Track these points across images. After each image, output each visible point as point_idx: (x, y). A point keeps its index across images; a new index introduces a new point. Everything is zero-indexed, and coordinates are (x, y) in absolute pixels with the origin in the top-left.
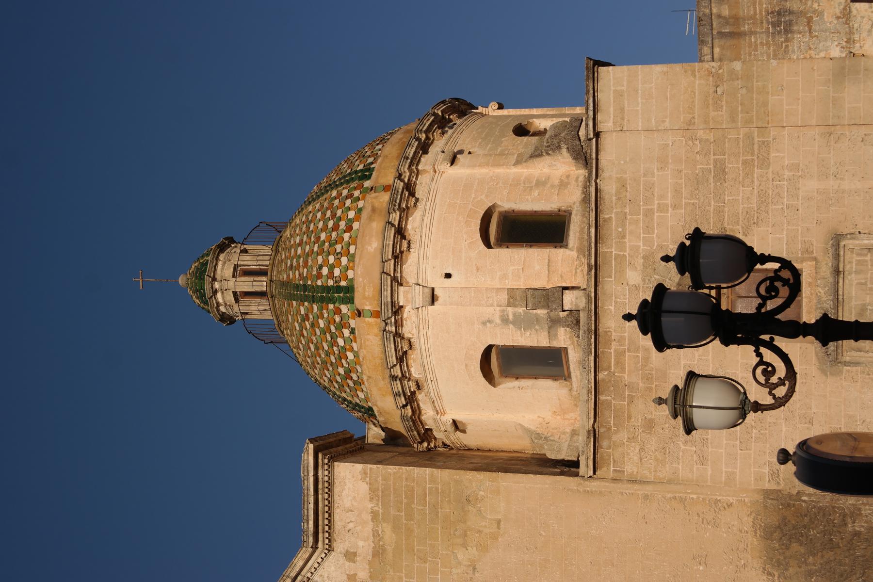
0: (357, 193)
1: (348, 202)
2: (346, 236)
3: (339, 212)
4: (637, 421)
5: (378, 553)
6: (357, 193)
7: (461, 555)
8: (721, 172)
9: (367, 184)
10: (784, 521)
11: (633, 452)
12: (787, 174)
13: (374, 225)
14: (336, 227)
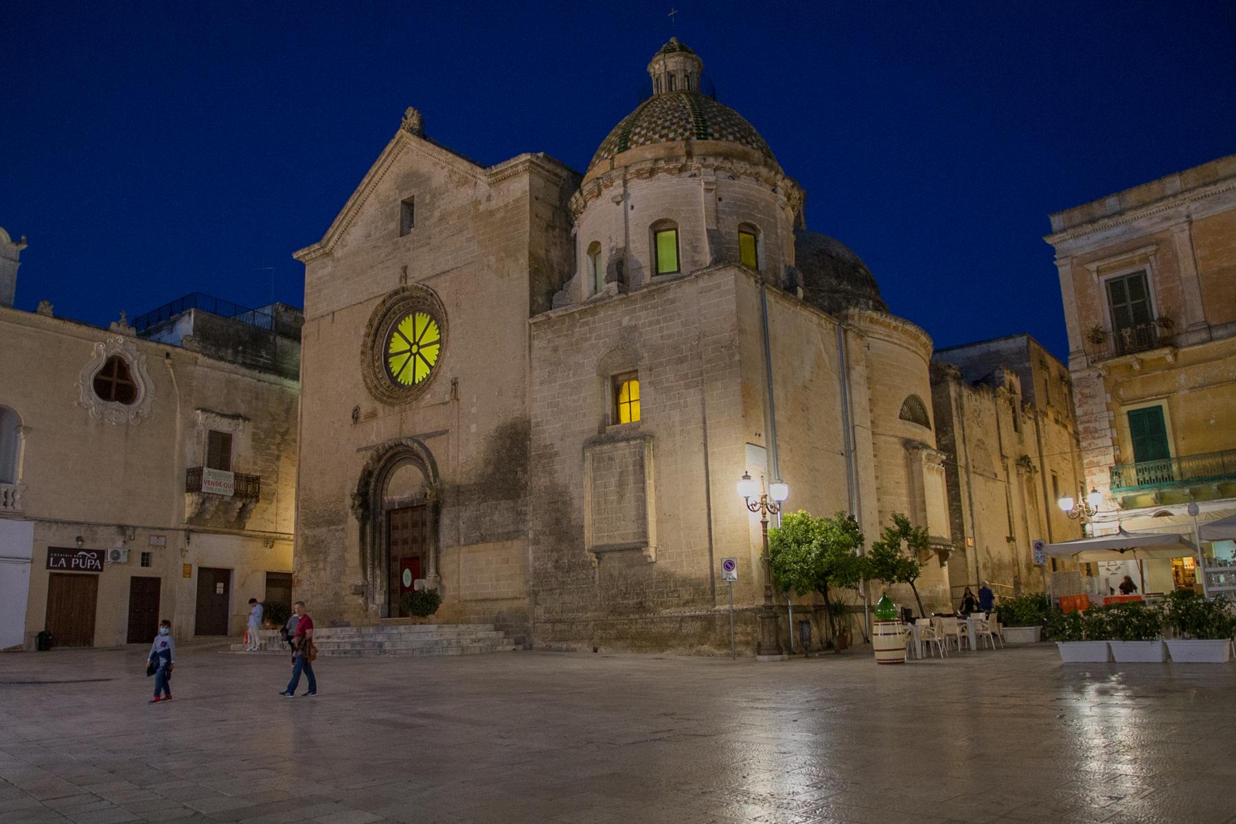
0: (687, 134)
1: (680, 131)
2: (657, 136)
3: (673, 127)
5: (491, 213)
6: (687, 134)
7: (492, 259)
8: (681, 361)
9: (694, 138)
12: (682, 401)
13: (662, 152)
14: (664, 128)
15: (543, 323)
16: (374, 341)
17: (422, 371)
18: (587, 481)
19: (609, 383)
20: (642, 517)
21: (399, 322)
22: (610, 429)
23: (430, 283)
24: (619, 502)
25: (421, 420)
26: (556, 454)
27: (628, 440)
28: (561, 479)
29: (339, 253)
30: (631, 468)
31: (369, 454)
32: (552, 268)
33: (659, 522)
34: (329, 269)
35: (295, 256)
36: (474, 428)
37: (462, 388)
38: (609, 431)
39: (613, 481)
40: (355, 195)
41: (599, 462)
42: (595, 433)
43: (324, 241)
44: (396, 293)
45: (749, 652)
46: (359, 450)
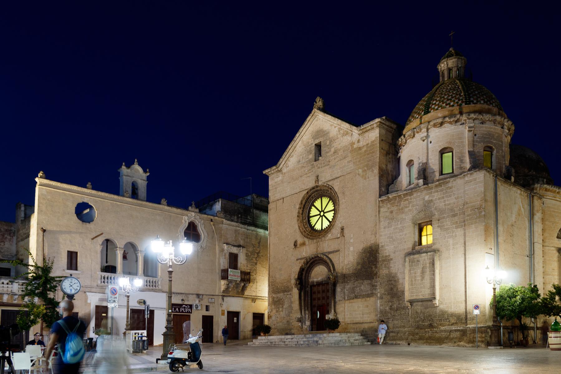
4: (392, 209)
10: (373, 251)
11: (385, 210)
15: (386, 200)
16: (303, 211)
17: (326, 224)
18: (407, 271)
19: (417, 227)
20: (433, 287)
21: (314, 201)
22: (417, 248)
23: (330, 183)
24: (422, 280)
25: (326, 245)
26: (391, 259)
27: (427, 252)
28: (393, 270)
29: (285, 170)
30: (428, 265)
31: (302, 261)
32: (388, 174)
33: (441, 289)
34: (280, 178)
35: (264, 173)
36: (352, 249)
37: (346, 231)
38: (417, 248)
39: (419, 271)
40: (293, 142)
41: (412, 263)
42: (411, 250)
43: (278, 165)
44: (313, 188)
45: (483, 345)
46: (297, 260)
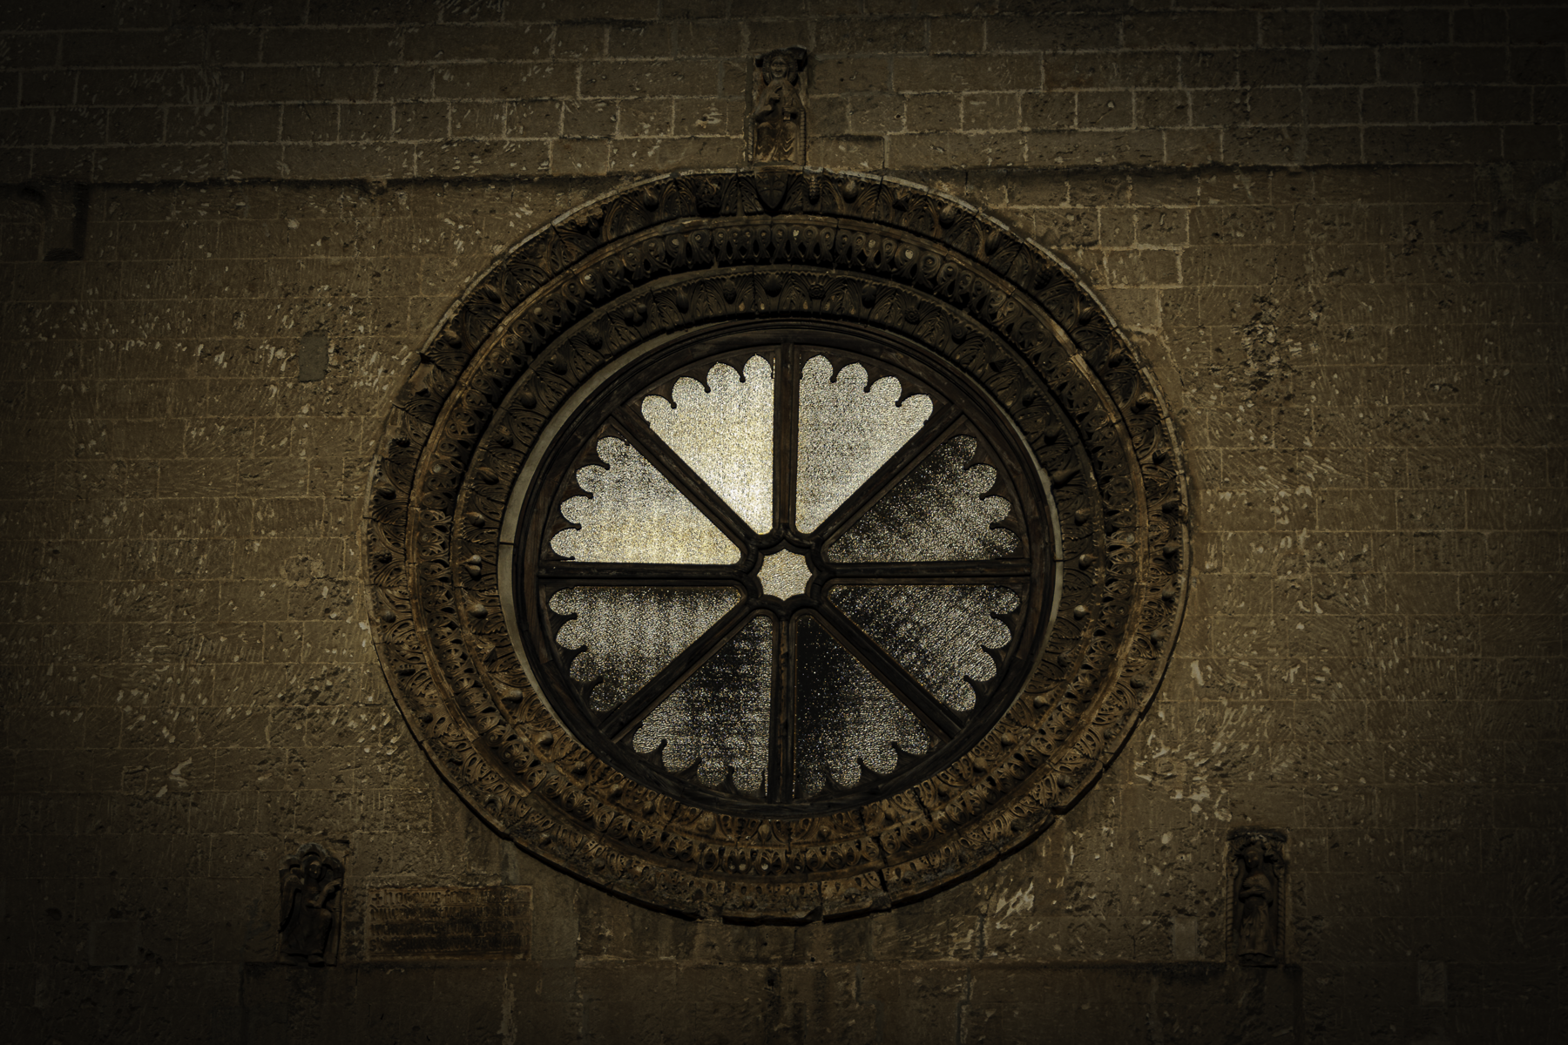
16: (464, 452)
44: (704, 198)
